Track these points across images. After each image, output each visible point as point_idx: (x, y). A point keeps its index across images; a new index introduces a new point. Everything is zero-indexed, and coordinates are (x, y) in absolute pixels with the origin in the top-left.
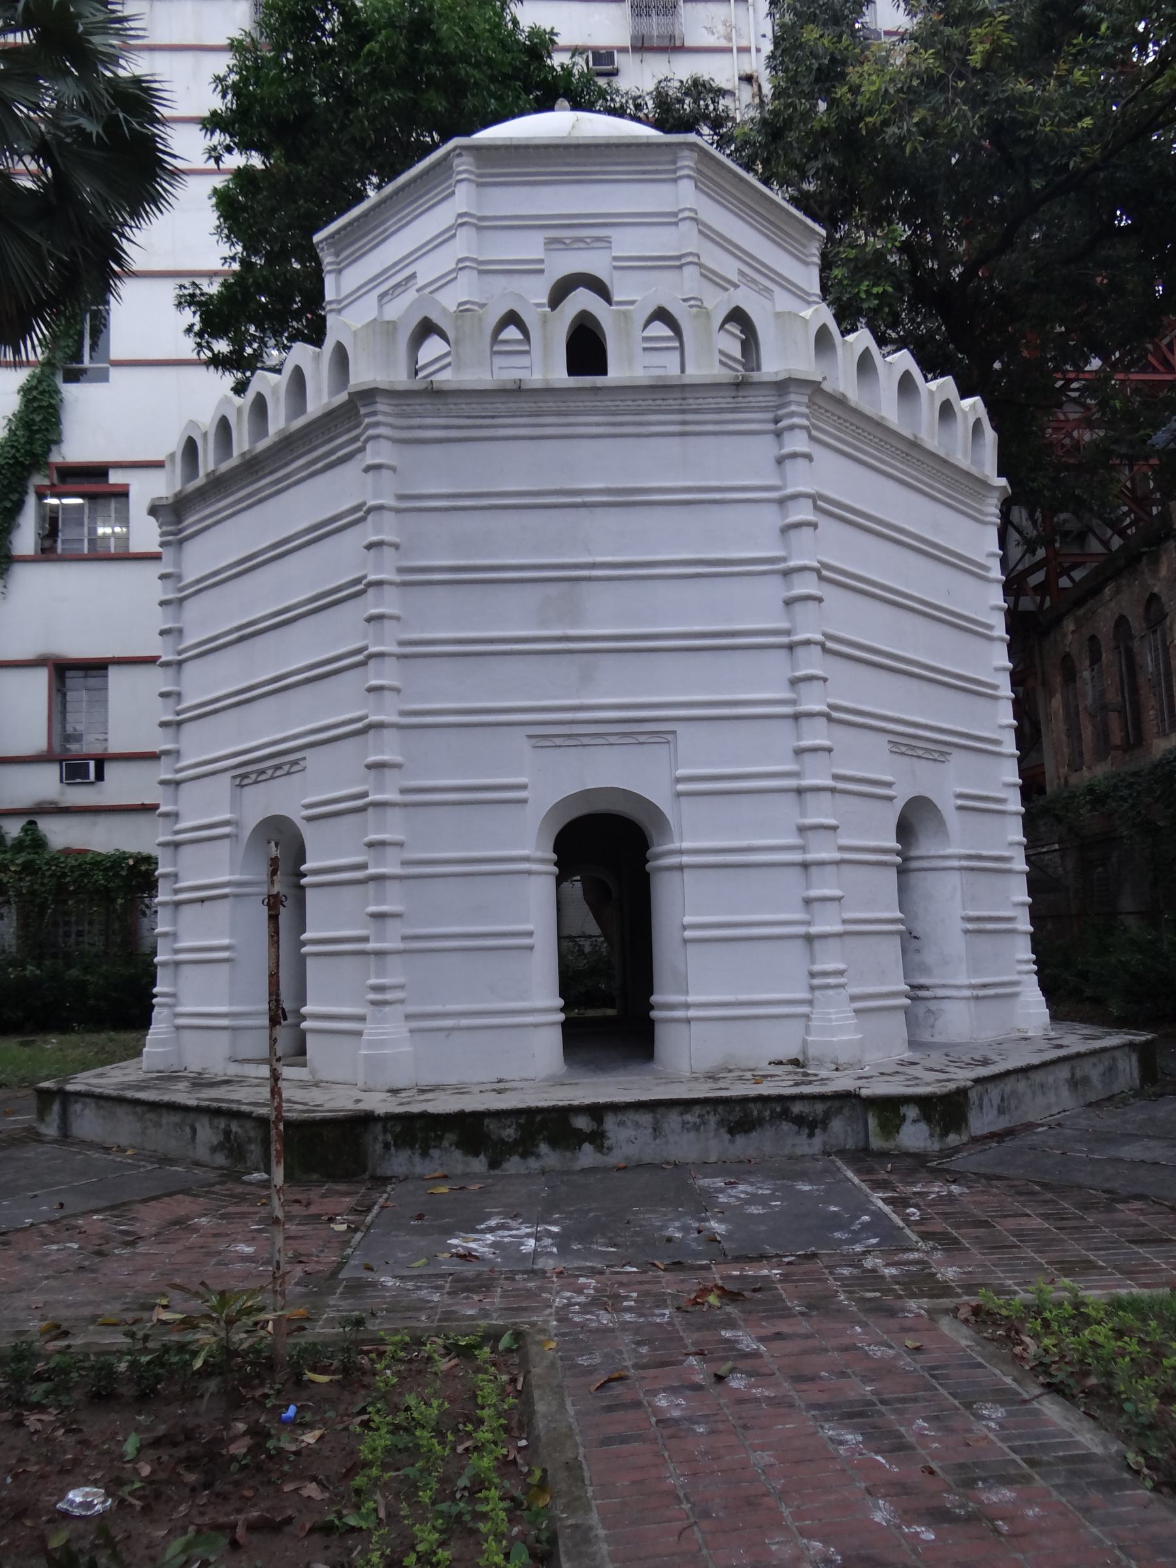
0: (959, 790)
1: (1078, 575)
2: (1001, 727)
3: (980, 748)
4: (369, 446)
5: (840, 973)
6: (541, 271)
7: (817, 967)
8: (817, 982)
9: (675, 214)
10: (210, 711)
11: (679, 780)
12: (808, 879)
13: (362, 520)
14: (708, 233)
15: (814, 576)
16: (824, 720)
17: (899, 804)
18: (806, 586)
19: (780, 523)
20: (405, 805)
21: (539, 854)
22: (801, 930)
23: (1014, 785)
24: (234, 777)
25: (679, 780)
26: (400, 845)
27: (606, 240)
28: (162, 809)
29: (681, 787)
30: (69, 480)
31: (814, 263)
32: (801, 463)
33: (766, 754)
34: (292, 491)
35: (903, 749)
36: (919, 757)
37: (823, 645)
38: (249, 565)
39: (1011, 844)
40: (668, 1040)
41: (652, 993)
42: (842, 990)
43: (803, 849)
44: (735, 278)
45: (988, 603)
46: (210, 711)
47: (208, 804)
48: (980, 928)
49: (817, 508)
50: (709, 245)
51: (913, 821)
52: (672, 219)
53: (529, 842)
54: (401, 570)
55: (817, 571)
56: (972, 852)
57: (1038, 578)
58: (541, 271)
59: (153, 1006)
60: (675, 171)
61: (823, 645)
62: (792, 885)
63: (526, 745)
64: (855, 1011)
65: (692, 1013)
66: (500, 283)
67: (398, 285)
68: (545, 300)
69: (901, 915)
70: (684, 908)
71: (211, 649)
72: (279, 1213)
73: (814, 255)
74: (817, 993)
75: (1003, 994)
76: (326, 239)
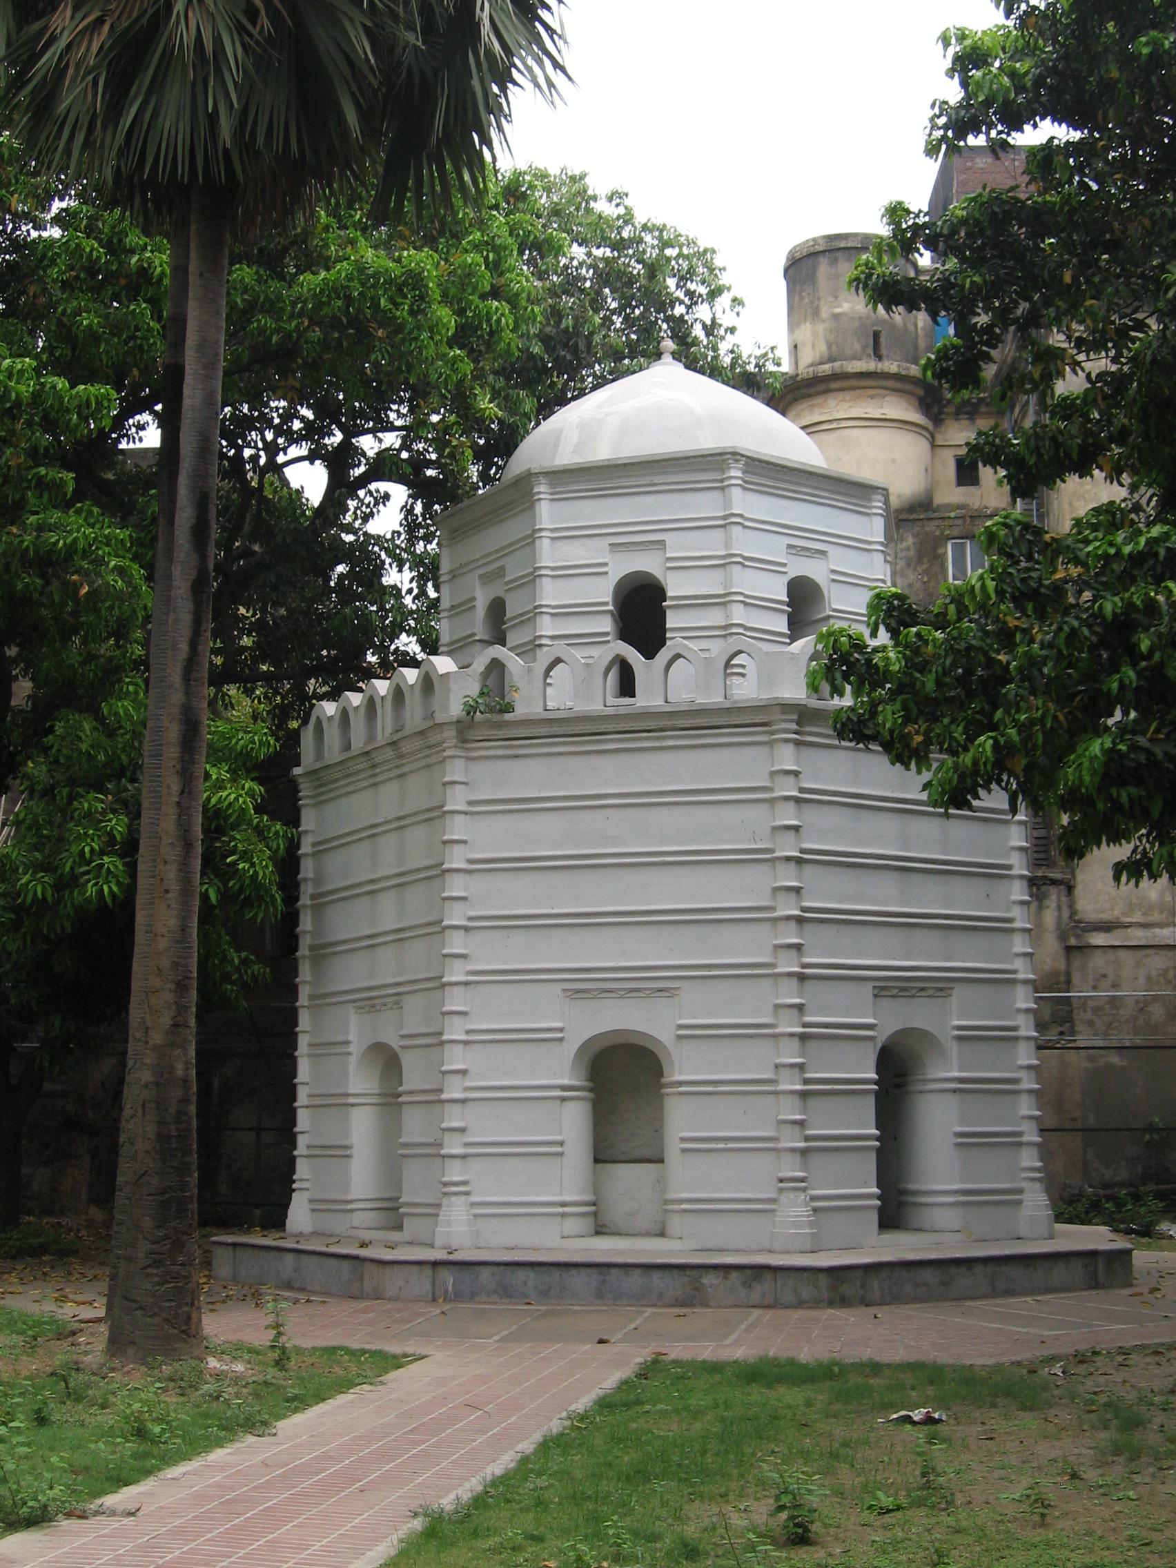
17: (879, 1045)
60: (722, 481)
68: (609, 599)
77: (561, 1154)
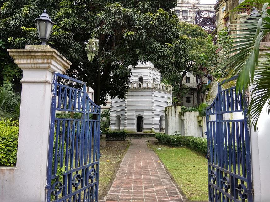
40: (143, 131)
53: (135, 118)
57: (200, 85)
62: (151, 121)
70: (145, 122)
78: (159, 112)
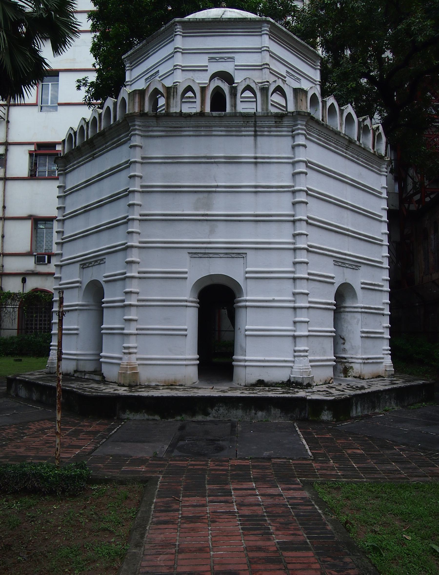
0: (363, 281)
1: (432, 196)
2: (383, 257)
3: (373, 265)
4: (132, 138)
5: (306, 351)
6: (207, 70)
7: (297, 348)
8: (296, 354)
9: (261, 49)
10: (73, 239)
11: (247, 273)
12: (295, 313)
13: (129, 167)
14: (273, 56)
15: (305, 194)
16: (305, 251)
17: (336, 286)
18: (302, 197)
19: (292, 172)
20: (140, 278)
21: (192, 299)
22: (291, 333)
23: (387, 280)
24: (81, 265)
25: (247, 273)
26: (137, 293)
27: (233, 58)
28: (56, 276)
29: (247, 275)
30: (41, 149)
31: (318, 69)
32: (302, 149)
33: (282, 264)
34: (105, 155)
35: (340, 264)
36: (347, 267)
37: (307, 221)
38: (88, 184)
39: (384, 303)
41: (234, 355)
42: (306, 358)
43: (294, 302)
44: (284, 74)
45: (380, 207)
46: (73, 239)
47: (72, 275)
48: (368, 336)
49: (307, 166)
50: (274, 61)
51: (343, 293)
52: (260, 50)
54: (142, 187)
55: (306, 192)
56: (367, 306)
57: (417, 197)
58: (207, 70)
59: (50, 350)
60: (261, 32)
61: (307, 221)
62: (289, 315)
63: (187, 257)
64: (311, 366)
65: (247, 364)
66: (190, 75)
67: (152, 75)
68: (208, 82)
69: (334, 329)
70: (249, 322)
71: (74, 215)
72: (58, 430)
73: (319, 65)
74: (296, 359)
75: (376, 362)
76: (126, 57)
77: (186, 335)
78: (331, 261)
